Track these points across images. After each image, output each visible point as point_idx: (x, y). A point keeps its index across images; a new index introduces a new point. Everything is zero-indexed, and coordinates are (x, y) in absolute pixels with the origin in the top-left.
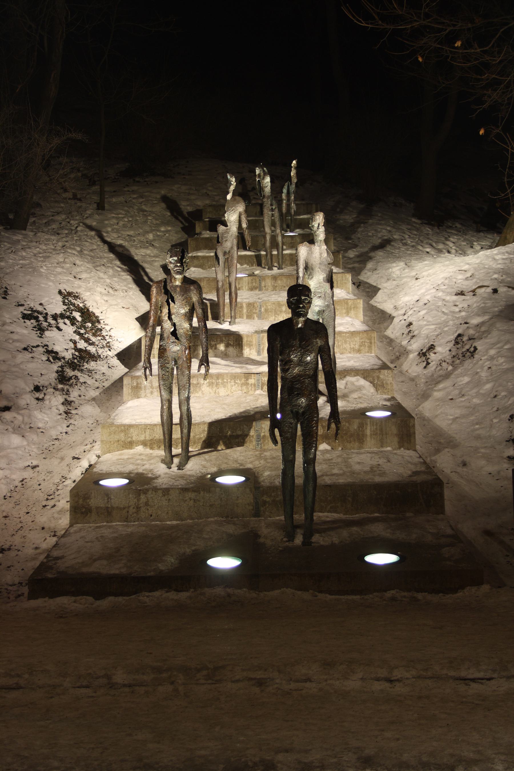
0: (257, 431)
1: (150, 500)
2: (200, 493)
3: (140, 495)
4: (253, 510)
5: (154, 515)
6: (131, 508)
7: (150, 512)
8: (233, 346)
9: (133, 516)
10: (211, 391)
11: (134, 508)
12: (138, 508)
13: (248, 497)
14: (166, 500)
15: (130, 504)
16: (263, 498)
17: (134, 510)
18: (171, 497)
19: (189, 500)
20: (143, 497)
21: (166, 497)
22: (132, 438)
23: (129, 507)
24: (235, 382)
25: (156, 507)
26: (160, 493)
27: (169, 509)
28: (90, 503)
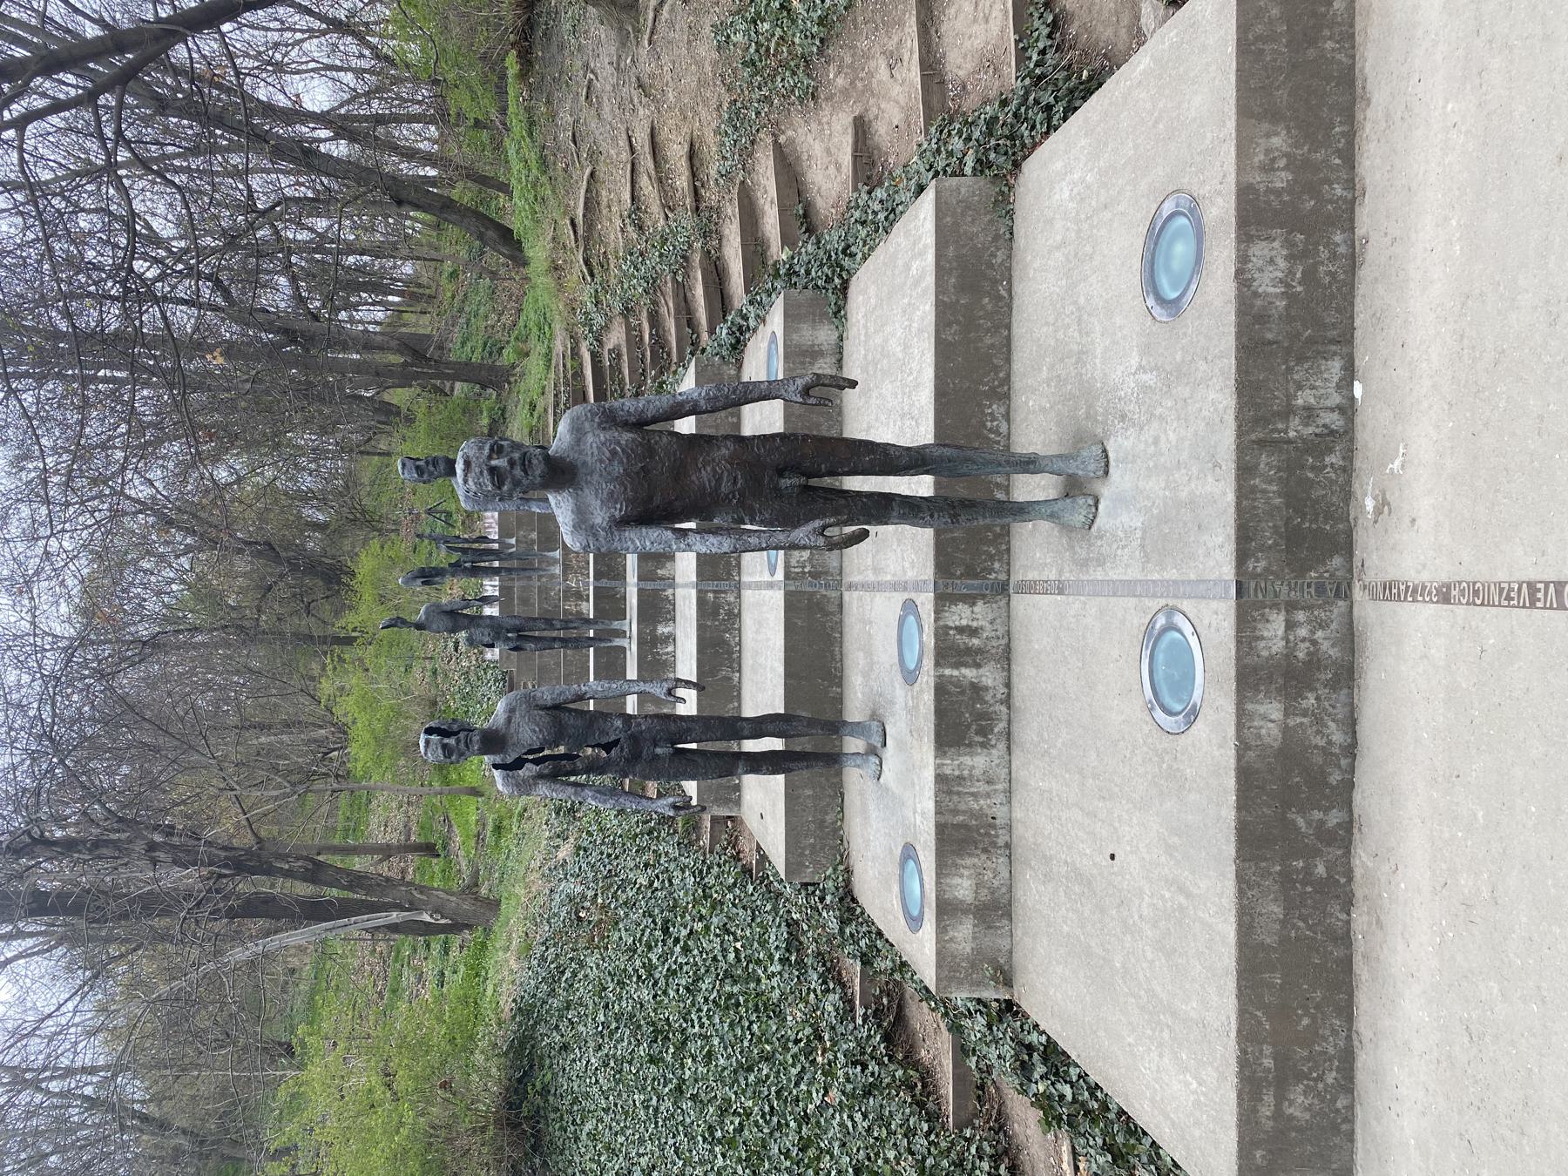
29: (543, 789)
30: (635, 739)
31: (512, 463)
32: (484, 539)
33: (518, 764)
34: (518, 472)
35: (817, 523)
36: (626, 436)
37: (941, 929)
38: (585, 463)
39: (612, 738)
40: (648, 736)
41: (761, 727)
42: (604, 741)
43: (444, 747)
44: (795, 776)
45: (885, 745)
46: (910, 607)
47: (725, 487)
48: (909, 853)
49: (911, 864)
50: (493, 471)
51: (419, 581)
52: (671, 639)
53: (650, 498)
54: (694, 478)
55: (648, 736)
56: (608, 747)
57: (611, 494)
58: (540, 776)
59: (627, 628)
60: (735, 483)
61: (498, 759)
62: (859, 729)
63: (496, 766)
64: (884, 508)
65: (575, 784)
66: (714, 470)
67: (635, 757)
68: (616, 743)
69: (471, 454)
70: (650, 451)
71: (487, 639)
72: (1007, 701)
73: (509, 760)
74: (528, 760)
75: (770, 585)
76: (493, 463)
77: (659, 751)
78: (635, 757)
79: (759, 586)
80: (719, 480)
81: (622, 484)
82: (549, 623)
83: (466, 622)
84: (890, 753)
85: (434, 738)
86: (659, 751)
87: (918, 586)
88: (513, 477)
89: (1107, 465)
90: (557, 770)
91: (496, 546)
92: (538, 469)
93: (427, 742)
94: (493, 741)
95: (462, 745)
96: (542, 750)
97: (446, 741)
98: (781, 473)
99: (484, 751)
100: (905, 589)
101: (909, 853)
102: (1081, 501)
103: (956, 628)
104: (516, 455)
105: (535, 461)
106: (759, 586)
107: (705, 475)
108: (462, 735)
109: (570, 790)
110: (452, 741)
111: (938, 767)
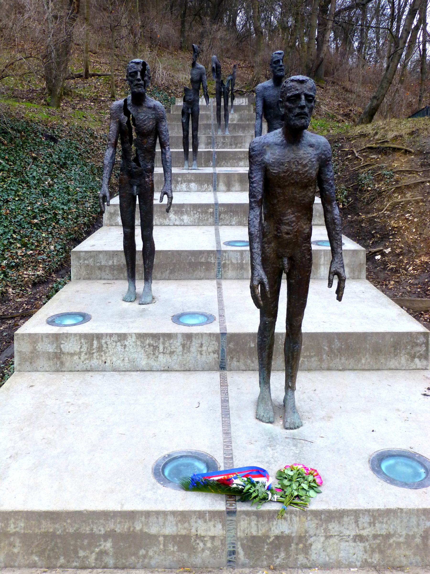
0: (218, 258)
1: (105, 346)
2: (159, 339)
3: (93, 340)
4: (218, 358)
5: (108, 362)
6: (83, 354)
7: (104, 358)
8: (194, 182)
9: (85, 363)
10: (176, 218)
11: (86, 354)
12: (90, 353)
13: (214, 344)
14: (122, 345)
15: (82, 350)
16: (230, 345)
17: (86, 357)
18: (127, 343)
19: (147, 347)
20: (95, 342)
21: (122, 342)
22: (101, 263)
23: (80, 353)
24: (196, 211)
25: (111, 353)
26: (115, 338)
27: (125, 356)
28: (37, 347)
29: (114, 127)
30: (141, 175)
31: (303, 107)
32: (233, 99)
33: (127, 113)
34: (297, 111)
35: (266, 280)
36: (314, 173)
37: (48, 336)
38: (299, 149)
39: (141, 163)
40: (143, 182)
41: (148, 239)
42: (140, 159)
43: (136, 73)
44: (123, 255)
45: (140, 304)
46: (209, 319)
48: (85, 317)
49: (81, 319)
50: (298, 97)
51: (214, 65)
52: (189, 190)
53: (279, 187)
54: (289, 211)
55: (143, 182)
56: (136, 160)
57: (282, 164)
58: (120, 124)
59: (193, 168)
60: (288, 234)
61: (129, 102)
62: (148, 290)
63: (126, 101)
64: (268, 312)
65: (116, 143)
66: (293, 222)
67: (131, 175)
68: (139, 165)
69: (308, 84)
70: (306, 187)
73: (129, 108)
74: (129, 117)
75: (218, 243)
76: (303, 97)
77: (135, 187)
79: (217, 234)
80: (288, 224)
81: (288, 170)
82: (195, 129)
83: (197, 88)
84: (135, 306)
85: (140, 67)
86: (135, 187)
87: (222, 323)
88: (295, 108)
89: (291, 429)
90: (123, 133)
91: (230, 104)
92: (299, 123)
93: (138, 63)
94: (138, 99)
95: (136, 82)
96: (134, 124)
97: (139, 73)
99: (134, 95)
100: (220, 316)
101: (85, 317)
102: (272, 414)
103: (202, 344)
104: (306, 110)
105: (303, 121)
106: (217, 234)
107: (291, 217)
108: (142, 82)
109: (113, 141)
110: (139, 77)
111: (131, 335)
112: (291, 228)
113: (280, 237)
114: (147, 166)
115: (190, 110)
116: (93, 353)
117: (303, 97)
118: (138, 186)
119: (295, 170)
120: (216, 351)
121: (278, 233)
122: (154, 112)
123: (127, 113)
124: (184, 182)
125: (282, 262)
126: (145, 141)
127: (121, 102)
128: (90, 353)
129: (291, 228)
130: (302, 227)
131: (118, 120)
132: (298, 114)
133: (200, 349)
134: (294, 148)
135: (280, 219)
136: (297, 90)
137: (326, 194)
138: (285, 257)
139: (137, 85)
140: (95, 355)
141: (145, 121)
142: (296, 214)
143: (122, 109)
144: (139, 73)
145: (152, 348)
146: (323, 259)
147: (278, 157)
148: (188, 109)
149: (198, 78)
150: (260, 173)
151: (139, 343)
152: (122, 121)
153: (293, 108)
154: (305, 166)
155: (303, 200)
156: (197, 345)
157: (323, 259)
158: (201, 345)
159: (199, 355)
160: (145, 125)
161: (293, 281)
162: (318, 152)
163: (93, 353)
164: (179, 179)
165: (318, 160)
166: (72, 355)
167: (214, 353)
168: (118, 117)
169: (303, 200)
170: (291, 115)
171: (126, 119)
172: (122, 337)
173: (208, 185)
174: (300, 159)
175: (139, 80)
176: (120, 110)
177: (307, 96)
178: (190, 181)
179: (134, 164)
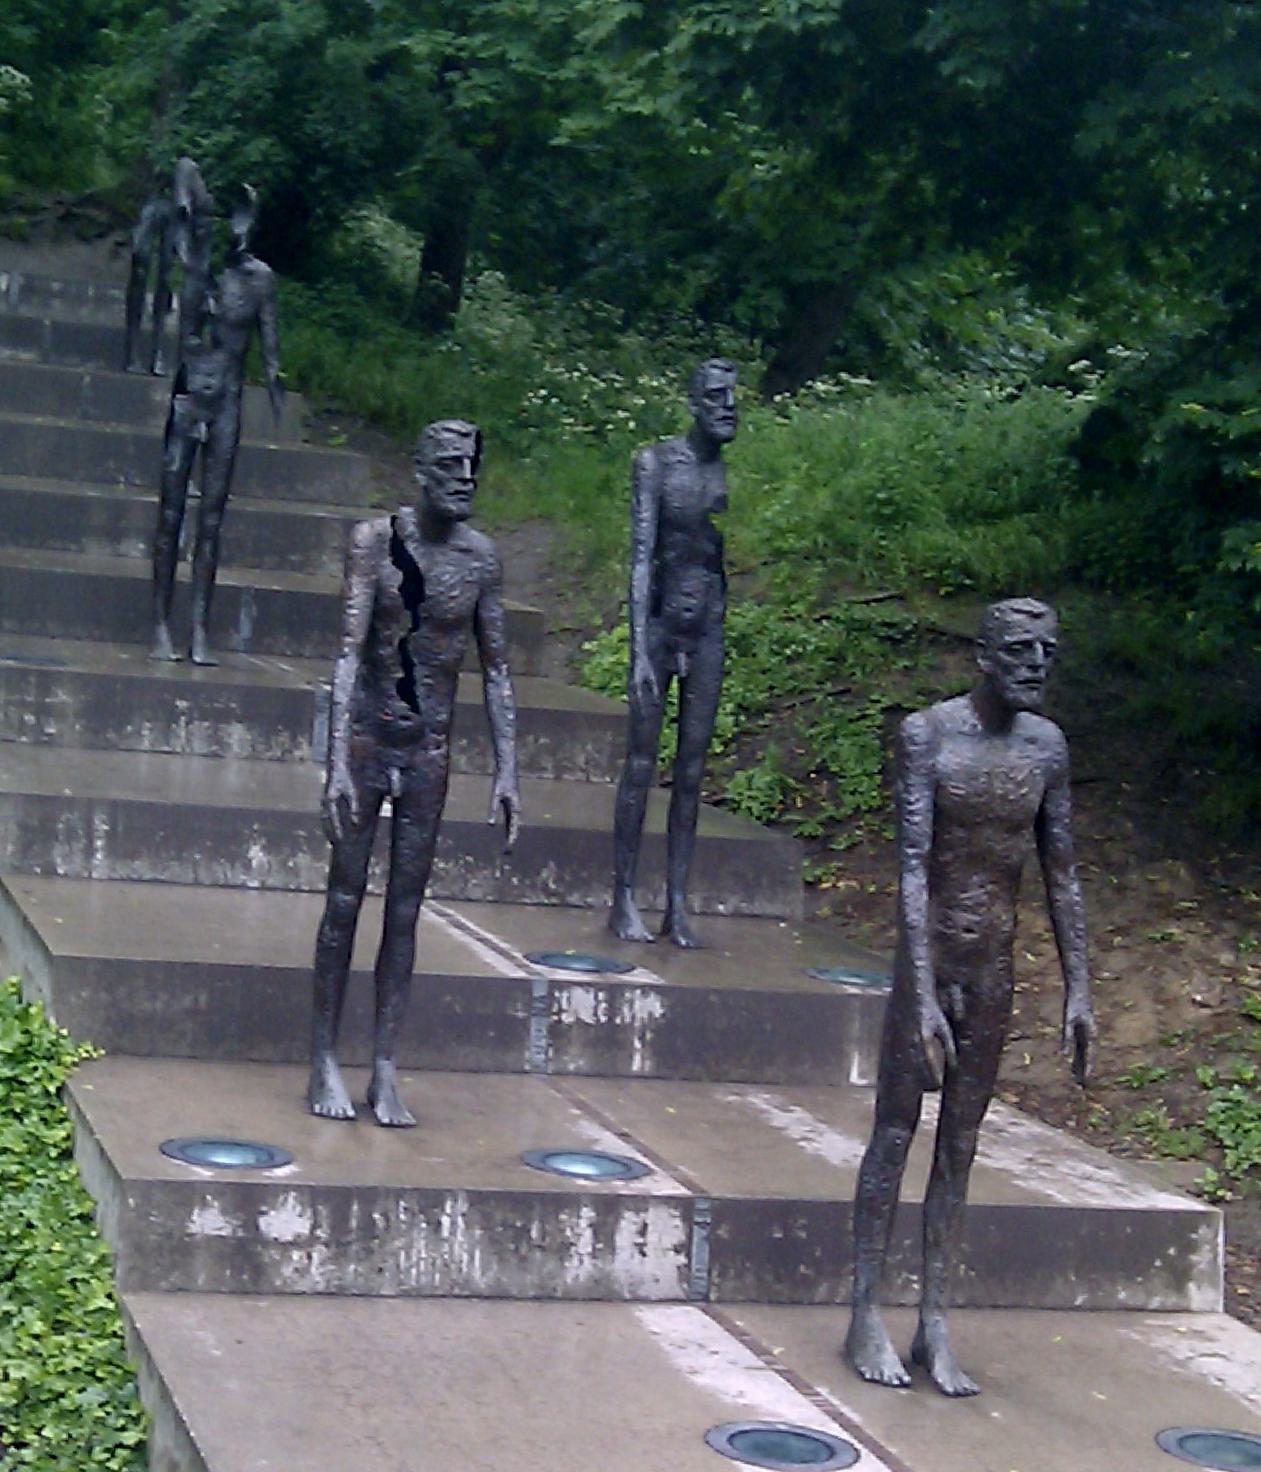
30: (414, 739)
31: (1034, 668)
33: (401, 557)
38: (1009, 747)
39: (423, 705)
41: (399, 932)
42: (420, 691)
43: (458, 460)
47: (965, 918)
50: (1028, 645)
58: (378, 591)
66: (982, 905)
68: (415, 708)
71: (196, 382)
72: (545, 1296)
73: (411, 547)
78: (388, 735)
85: (468, 446)
86: (396, 775)
97: (467, 462)
98: (966, 990)
103: (645, 1225)
112: (977, 918)
113: (949, 938)
114: (438, 713)
115: (203, 427)
116: (349, 1243)
117: (1039, 647)
118: (402, 770)
119: (999, 792)
120: (682, 1245)
121: (950, 928)
122: (476, 564)
123: (401, 557)
124: (203, 719)
125: (950, 995)
126: (443, 642)
127: (384, 523)
128: (339, 1244)
129: (977, 918)
130: (999, 918)
131: (374, 577)
132: (1027, 681)
133: (641, 1240)
134: (998, 742)
135: (955, 898)
136: (1028, 632)
137: (1057, 848)
138: (956, 983)
139: (457, 492)
140: (354, 1247)
141: (452, 587)
142: (990, 887)
143: (387, 546)
144: (467, 462)
145: (510, 1233)
146: (856, 1025)
147: (967, 762)
148: (195, 422)
149: (248, 310)
150: (927, 793)
151: (477, 1217)
152: (387, 583)
153: (1017, 666)
154: (1020, 785)
155: (1007, 857)
156: (634, 1228)
157: (856, 1025)
158: (643, 1232)
159: (638, 1256)
160: (453, 598)
161: (967, 1042)
162: (1046, 754)
163: (349, 1243)
164: (182, 704)
165: (1044, 773)
166: (287, 1246)
167: (677, 1251)
168: (374, 569)
169: (1007, 857)
170: (1009, 679)
171: (399, 576)
172: (430, 1202)
173: (294, 738)
174: (1012, 769)
175: (465, 481)
176: (381, 550)
177: (1045, 645)
178: (223, 717)
179: (404, 704)
